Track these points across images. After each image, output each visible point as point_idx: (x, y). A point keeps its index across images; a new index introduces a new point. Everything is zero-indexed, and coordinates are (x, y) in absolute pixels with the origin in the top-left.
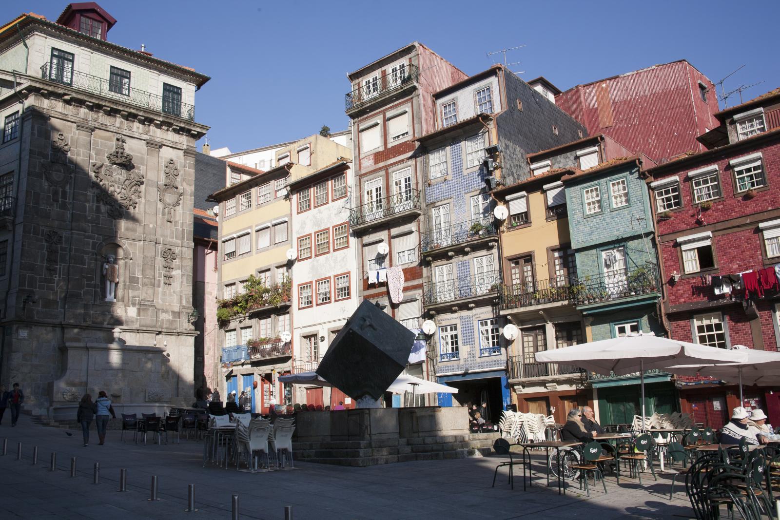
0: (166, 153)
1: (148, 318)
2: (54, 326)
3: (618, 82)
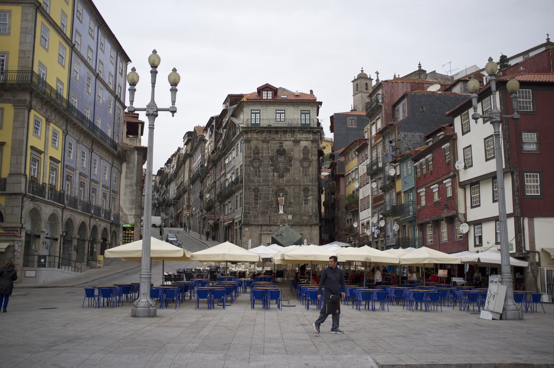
0: (303, 144)
1: (297, 219)
2: (258, 225)
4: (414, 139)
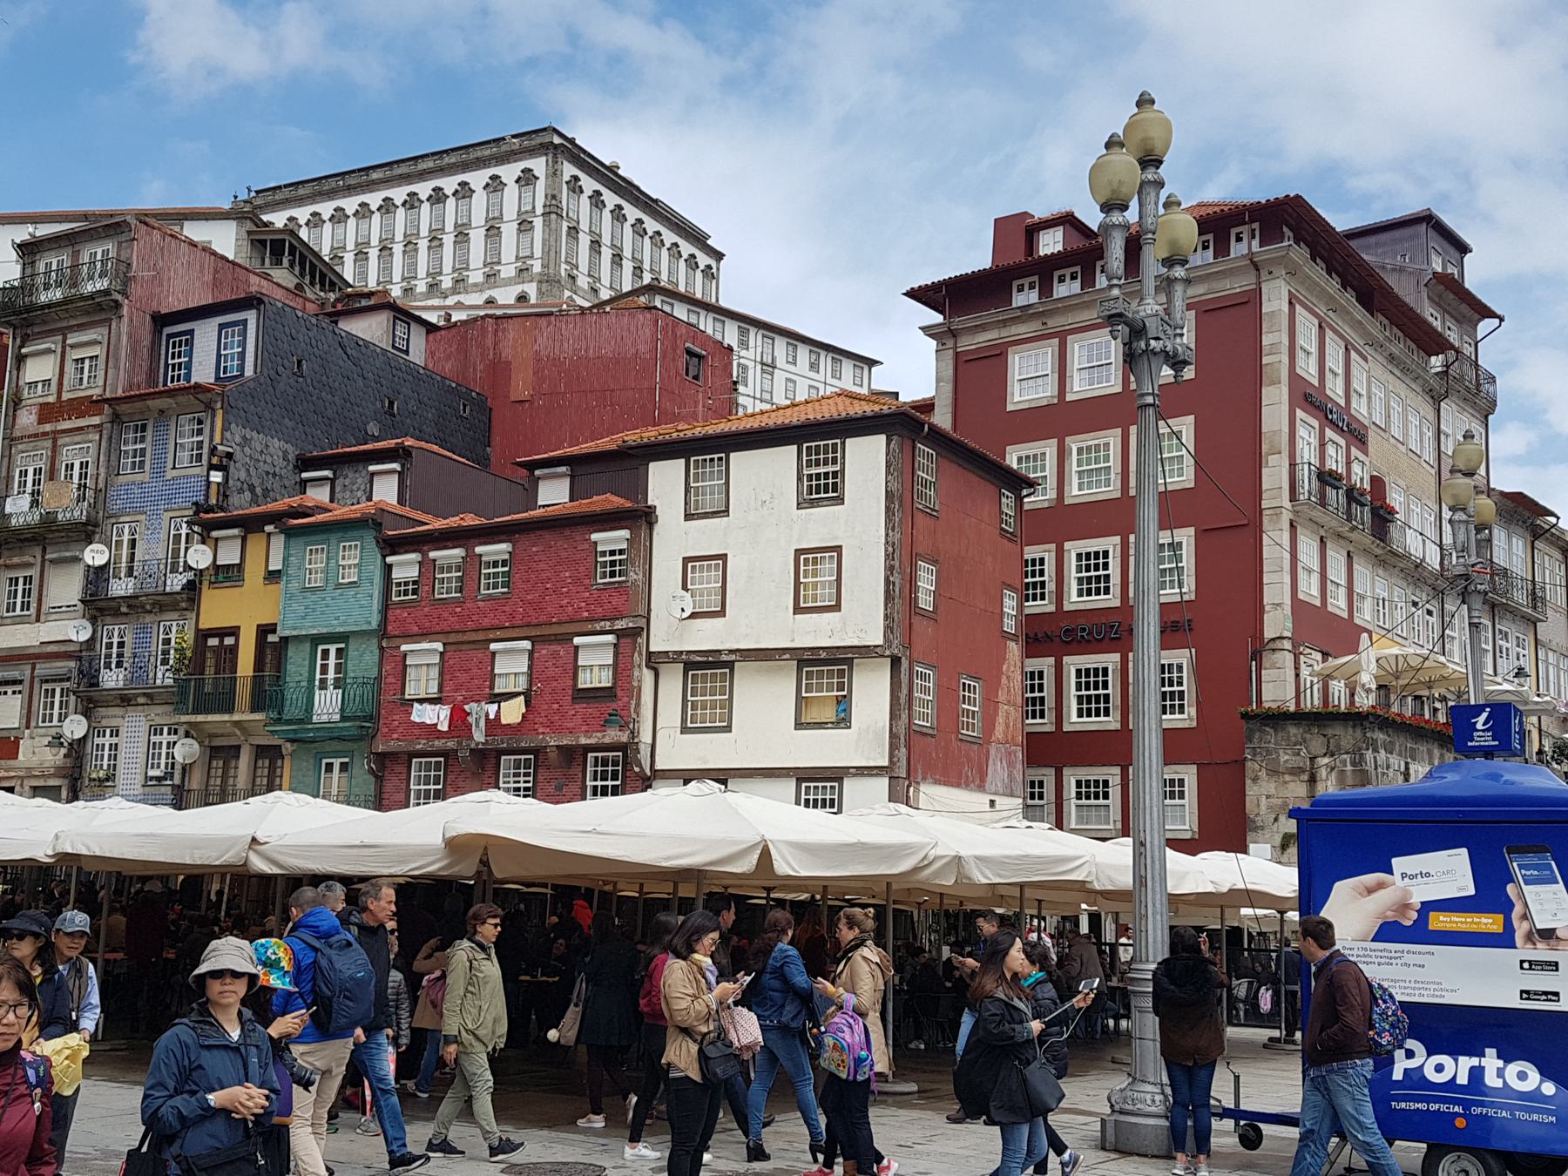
3: (549, 324)
4: (269, 460)
